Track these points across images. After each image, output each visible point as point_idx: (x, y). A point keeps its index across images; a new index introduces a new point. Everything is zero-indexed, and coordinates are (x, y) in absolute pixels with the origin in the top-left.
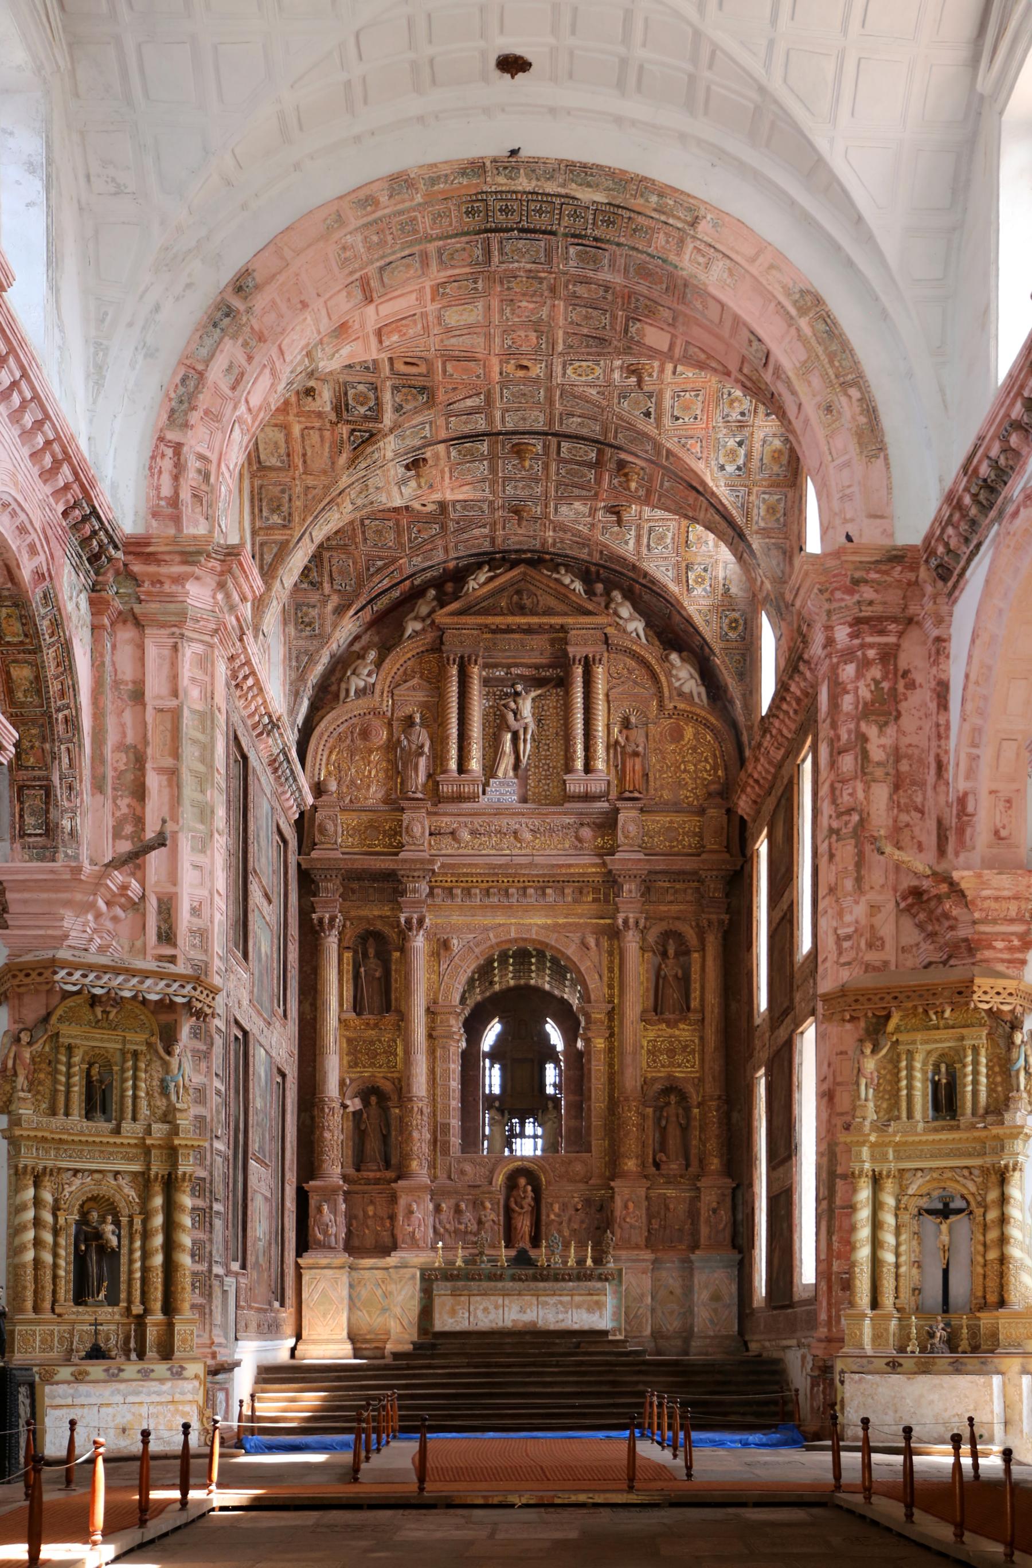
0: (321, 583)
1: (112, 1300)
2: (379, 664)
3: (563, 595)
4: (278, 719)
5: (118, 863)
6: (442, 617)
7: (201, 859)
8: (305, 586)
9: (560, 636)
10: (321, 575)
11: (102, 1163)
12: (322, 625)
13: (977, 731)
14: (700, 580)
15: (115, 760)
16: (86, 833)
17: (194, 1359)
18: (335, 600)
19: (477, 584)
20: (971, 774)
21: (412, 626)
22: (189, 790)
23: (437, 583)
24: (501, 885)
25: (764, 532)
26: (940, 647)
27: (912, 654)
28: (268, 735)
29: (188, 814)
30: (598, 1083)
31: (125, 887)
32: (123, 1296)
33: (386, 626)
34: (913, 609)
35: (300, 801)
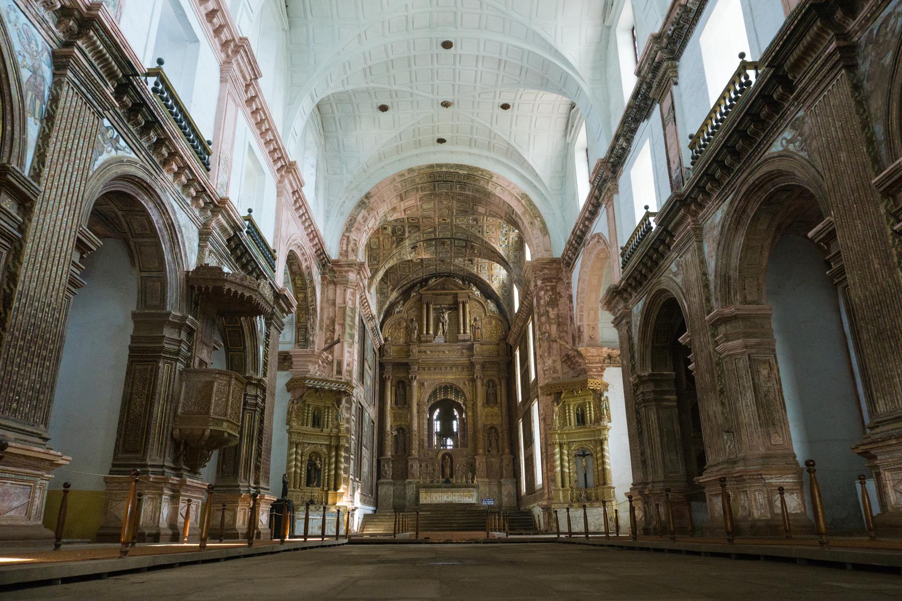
1: (318, 485)
2: (403, 305)
3: (456, 285)
5: (325, 350)
6: (421, 291)
7: (350, 350)
9: (456, 296)
11: (318, 441)
13: (582, 307)
14: (495, 279)
15: (326, 322)
16: (317, 341)
19: (432, 282)
20: (581, 320)
21: (413, 294)
22: (348, 330)
23: (420, 282)
24: (438, 366)
25: (514, 263)
26: (569, 284)
27: (560, 288)
29: (347, 337)
30: (470, 426)
31: (327, 357)
33: (405, 295)
34: (560, 275)
35: (380, 342)
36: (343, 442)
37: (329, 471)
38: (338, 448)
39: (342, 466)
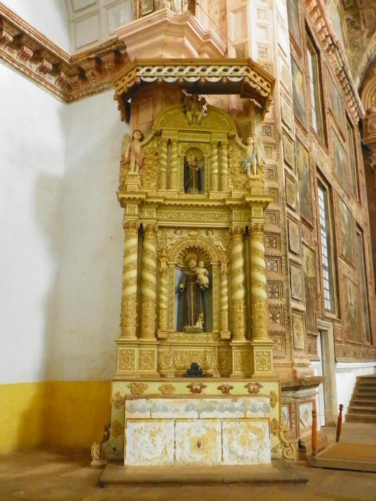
0: (360, 26)
4: (337, 43)
8: (353, 30)
10: (359, 23)
11: (198, 223)
12: (362, 44)
17: (270, 379)
18: (367, 31)
28: (333, 52)
32: (215, 324)
36: (258, 218)
37: (232, 290)
38: (247, 234)
39: (261, 277)
